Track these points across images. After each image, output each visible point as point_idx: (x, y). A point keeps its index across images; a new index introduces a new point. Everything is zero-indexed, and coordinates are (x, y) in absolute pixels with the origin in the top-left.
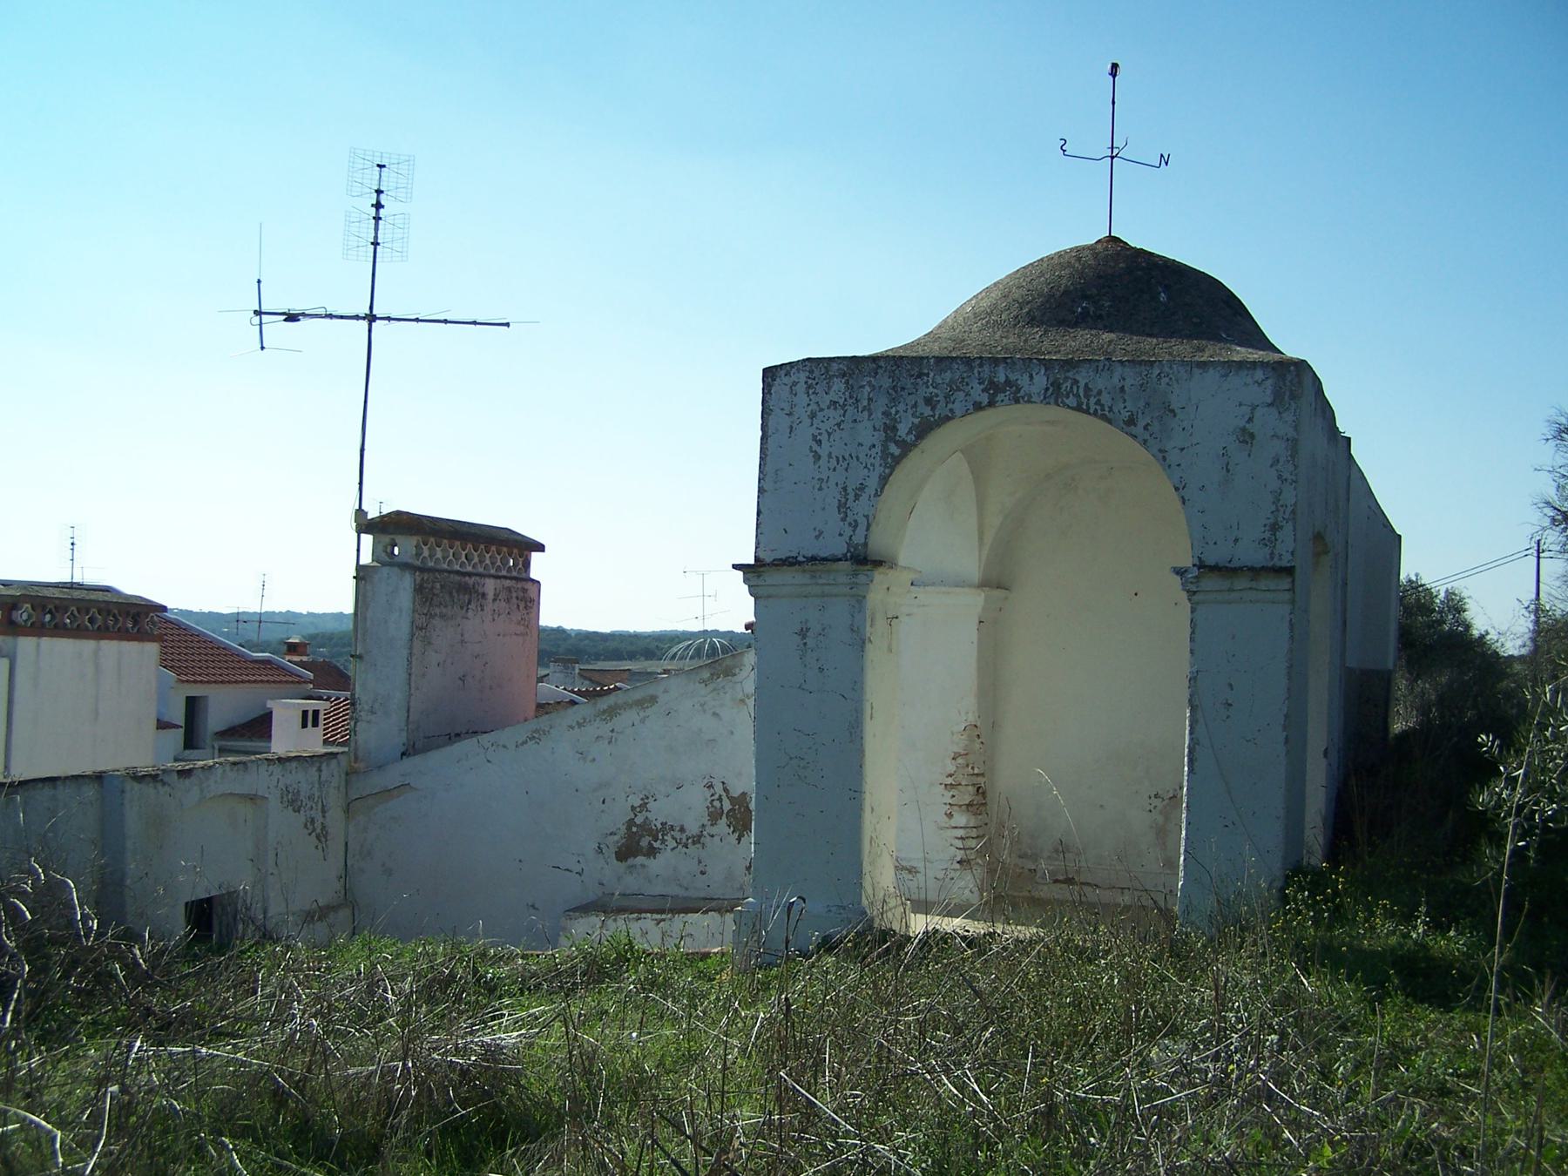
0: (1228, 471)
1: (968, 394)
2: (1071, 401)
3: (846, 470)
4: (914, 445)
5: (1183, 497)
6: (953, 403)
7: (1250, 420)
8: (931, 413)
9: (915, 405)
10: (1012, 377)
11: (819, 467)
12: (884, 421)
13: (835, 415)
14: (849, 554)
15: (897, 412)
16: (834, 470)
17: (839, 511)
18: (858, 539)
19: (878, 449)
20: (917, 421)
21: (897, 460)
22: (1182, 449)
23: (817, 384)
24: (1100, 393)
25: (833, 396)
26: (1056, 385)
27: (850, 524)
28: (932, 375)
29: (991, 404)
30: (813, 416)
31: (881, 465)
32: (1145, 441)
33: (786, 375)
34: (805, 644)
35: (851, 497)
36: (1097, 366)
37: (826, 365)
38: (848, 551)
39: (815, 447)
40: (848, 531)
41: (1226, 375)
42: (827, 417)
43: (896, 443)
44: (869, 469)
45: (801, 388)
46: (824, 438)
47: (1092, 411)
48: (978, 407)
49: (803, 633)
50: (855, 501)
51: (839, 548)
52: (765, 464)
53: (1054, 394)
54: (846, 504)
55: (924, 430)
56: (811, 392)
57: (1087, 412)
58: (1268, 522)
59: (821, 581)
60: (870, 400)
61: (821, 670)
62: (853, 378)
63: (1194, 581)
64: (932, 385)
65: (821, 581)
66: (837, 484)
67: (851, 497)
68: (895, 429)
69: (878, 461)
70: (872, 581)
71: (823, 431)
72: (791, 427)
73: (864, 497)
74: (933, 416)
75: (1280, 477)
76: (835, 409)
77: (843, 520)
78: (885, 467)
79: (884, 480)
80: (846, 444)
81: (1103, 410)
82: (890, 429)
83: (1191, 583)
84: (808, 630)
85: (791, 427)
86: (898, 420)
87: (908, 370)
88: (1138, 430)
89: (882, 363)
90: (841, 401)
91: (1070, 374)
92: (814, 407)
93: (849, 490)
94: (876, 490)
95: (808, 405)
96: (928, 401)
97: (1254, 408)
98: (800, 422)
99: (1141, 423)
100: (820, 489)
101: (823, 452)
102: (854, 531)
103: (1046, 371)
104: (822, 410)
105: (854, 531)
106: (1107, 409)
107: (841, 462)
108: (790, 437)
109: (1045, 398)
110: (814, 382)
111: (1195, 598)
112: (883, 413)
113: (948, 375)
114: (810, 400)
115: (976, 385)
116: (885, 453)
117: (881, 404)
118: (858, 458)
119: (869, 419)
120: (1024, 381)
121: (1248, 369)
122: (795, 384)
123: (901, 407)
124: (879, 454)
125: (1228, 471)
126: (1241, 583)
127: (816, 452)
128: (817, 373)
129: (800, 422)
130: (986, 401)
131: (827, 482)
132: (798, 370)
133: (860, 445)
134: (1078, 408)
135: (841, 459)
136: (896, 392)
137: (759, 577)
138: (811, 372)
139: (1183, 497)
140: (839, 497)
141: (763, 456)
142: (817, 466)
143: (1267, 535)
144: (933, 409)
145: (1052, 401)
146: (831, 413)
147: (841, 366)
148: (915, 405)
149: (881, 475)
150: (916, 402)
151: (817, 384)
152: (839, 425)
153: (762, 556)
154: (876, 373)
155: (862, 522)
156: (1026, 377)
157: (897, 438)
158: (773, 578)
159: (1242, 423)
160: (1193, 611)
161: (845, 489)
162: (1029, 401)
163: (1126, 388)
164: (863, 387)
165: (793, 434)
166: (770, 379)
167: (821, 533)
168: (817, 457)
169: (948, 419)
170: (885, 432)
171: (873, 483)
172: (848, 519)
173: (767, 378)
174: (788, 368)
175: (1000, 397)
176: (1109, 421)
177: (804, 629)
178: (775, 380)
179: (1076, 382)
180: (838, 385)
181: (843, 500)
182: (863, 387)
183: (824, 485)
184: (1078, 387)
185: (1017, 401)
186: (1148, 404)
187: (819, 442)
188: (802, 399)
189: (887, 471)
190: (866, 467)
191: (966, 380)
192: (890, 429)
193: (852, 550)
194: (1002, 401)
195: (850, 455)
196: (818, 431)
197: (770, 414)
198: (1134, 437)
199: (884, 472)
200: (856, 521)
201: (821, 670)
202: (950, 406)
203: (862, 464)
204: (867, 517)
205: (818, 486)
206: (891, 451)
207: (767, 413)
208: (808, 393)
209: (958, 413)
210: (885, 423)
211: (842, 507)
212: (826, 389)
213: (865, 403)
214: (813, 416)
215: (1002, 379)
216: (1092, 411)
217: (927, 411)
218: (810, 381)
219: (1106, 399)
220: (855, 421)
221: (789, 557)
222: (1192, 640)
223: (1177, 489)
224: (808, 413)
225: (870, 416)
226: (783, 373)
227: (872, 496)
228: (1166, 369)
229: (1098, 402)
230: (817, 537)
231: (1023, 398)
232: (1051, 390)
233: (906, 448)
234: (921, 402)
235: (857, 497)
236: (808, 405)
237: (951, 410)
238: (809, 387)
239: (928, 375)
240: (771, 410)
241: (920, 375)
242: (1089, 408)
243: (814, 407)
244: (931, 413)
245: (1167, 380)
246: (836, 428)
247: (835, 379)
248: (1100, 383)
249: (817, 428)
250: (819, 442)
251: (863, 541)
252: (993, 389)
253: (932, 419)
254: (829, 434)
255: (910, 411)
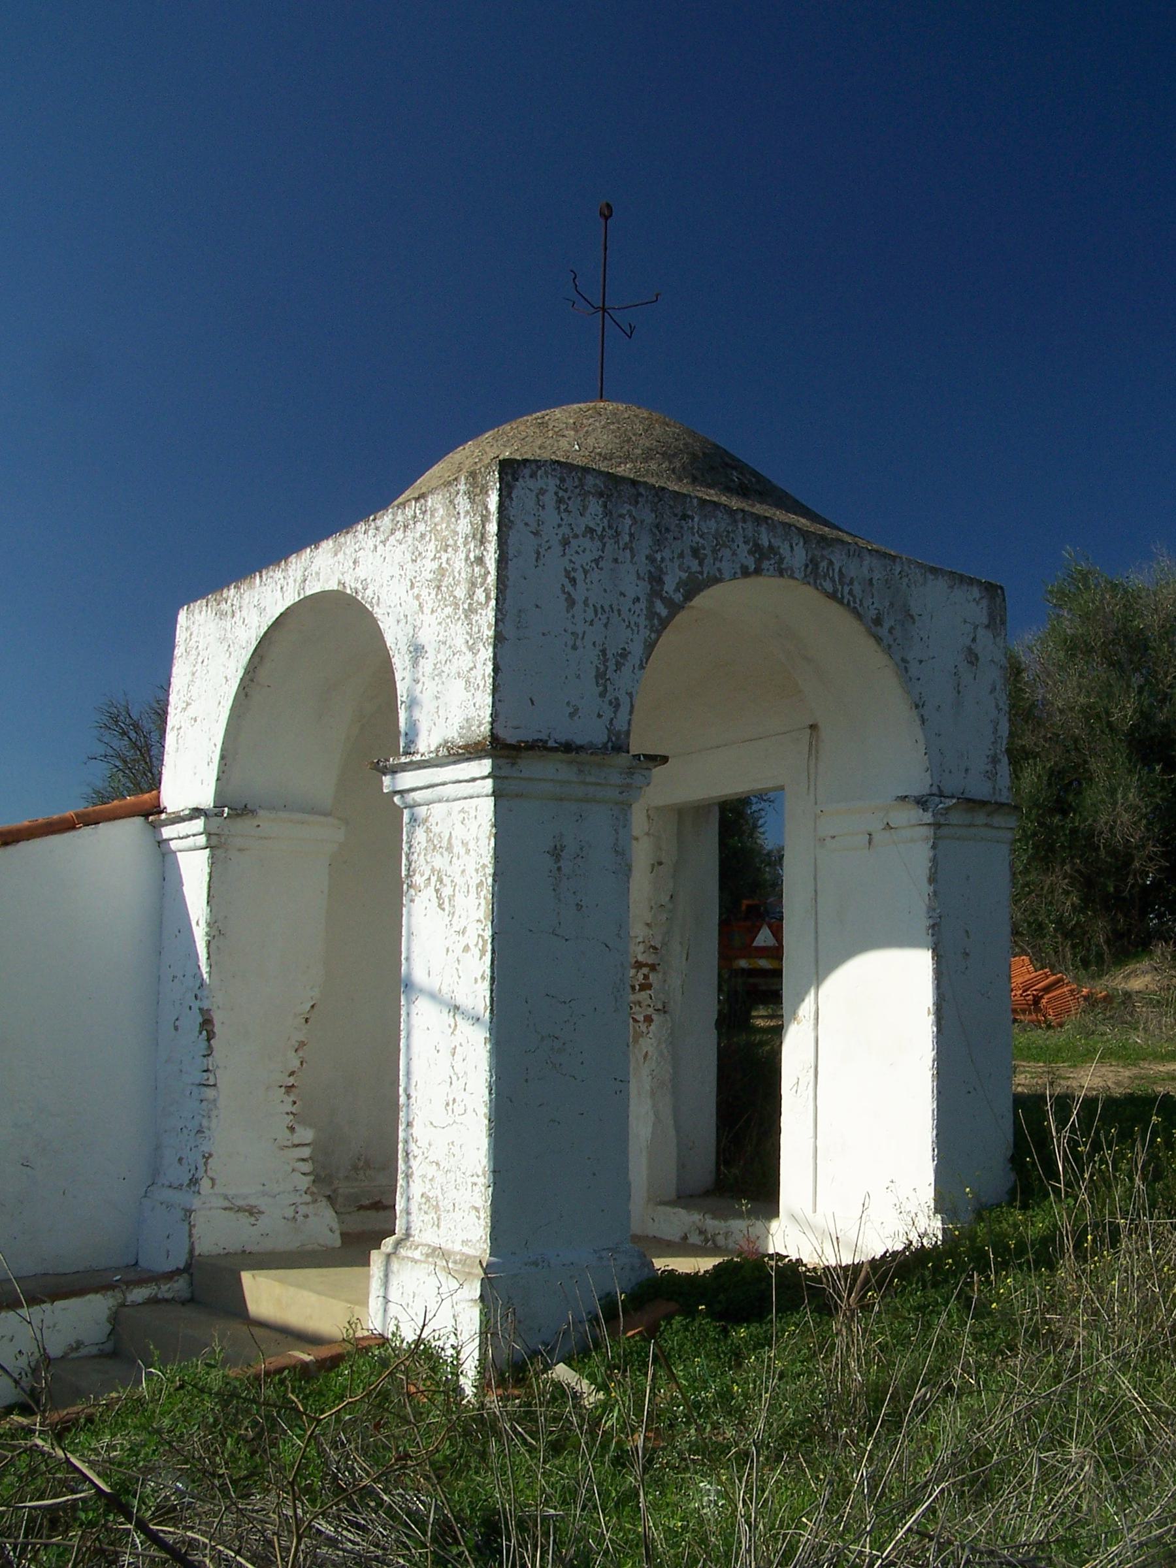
0: (959, 692)
1: (734, 554)
2: (828, 586)
3: (606, 625)
4: (681, 607)
5: (922, 716)
6: (721, 561)
7: (974, 640)
8: (699, 569)
9: (681, 555)
10: (776, 542)
11: (573, 617)
12: (649, 568)
13: (591, 547)
14: (610, 744)
15: (663, 559)
16: (591, 624)
17: (597, 683)
18: (620, 724)
19: (643, 604)
20: (684, 575)
21: (665, 623)
22: (921, 662)
23: (569, 498)
24: (851, 582)
25: (587, 521)
26: (814, 563)
27: (610, 703)
28: (696, 519)
29: (758, 571)
30: (565, 543)
31: (646, 627)
32: (890, 646)
33: (531, 477)
34: (559, 869)
35: (611, 665)
36: (849, 550)
37: (579, 474)
38: (610, 739)
39: (569, 588)
40: (608, 713)
41: (951, 587)
42: (582, 548)
43: (663, 599)
44: (632, 630)
45: (549, 499)
46: (579, 576)
47: (845, 601)
48: (746, 573)
49: (556, 853)
50: (616, 671)
51: (600, 737)
52: (505, 599)
53: (813, 573)
54: (605, 674)
55: (692, 588)
56: (563, 507)
57: (840, 602)
58: (989, 753)
59: (588, 779)
60: (631, 535)
61: (579, 907)
62: (611, 501)
63: (944, 812)
64: (698, 532)
65: (589, 779)
66: (594, 644)
67: (611, 665)
68: (660, 581)
69: (642, 621)
70: (648, 784)
71: (577, 566)
72: (538, 553)
73: (626, 670)
74: (701, 573)
75: (997, 706)
76: (592, 539)
77: (602, 695)
78: (652, 631)
79: (650, 646)
80: (605, 591)
81: (855, 602)
82: (656, 580)
83: (941, 814)
84: (563, 848)
85: (538, 553)
86: (665, 570)
87: (671, 507)
88: (883, 632)
89: (642, 490)
90: (599, 530)
91: (825, 553)
92: (565, 530)
93: (610, 655)
94: (641, 661)
95: (559, 526)
96: (695, 552)
97: (976, 627)
98: (549, 548)
99: (886, 626)
100: (574, 647)
101: (579, 595)
102: (615, 712)
103: (805, 543)
104: (576, 536)
105: (615, 712)
106: (858, 602)
107: (599, 615)
108: (536, 567)
109: (806, 576)
110: (566, 496)
111: (944, 831)
112: (647, 558)
113: (712, 524)
114: (562, 519)
115: (742, 545)
116: (652, 614)
117: (644, 544)
118: (619, 611)
119: (631, 562)
120: (784, 550)
121: (968, 584)
122: (542, 492)
123: (667, 553)
124: (645, 612)
125: (959, 692)
126: (981, 818)
127: (569, 594)
128: (569, 484)
129: (549, 548)
130: (752, 567)
131: (583, 638)
132: (546, 472)
133: (622, 594)
134: (833, 596)
135: (600, 610)
136: (660, 532)
137: (513, 764)
138: (562, 480)
139: (922, 716)
140: (596, 662)
141: (501, 586)
142: (570, 615)
143: (989, 767)
144: (701, 564)
145: (812, 581)
146: (586, 542)
147: (598, 482)
148: (681, 555)
149: (646, 641)
150: (682, 551)
151: (569, 498)
152: (597, 561)
153: (502, 734)
154: (637, 502)
155: (625, 700)
156: (787, 546)
157: (665, 595)
158: (533, 768)
159: (968, 642)
160: (934, 847)
161: (604, 652)
162: (792, 577)
163: (874, 582)
164: (622, 516)
165: (541, 563)
166: (510, 477)
167: (577, 710)
168: (571, 602)
169: (717, 580)
170: (650, 583)
171: (637, 649)
172: (608, 694)
173: (506, 474)
174: (534, 466)
175: (765, 564)
176: (859, 616)
177: (558, 847)
178: (517, 480)
179: (831, 563)
180: (595, 506)
181: (602, 668)
182: (622, 516)
183: (579, 643)
184: (833, 570)
185: (781, 573)
186: (892, 605)
187: (573, 581)
188: (551, 516)
189: (653, 636)
190: (628, 627)
191: (731, 535)
192: (656, 580)
193: (614, 739)
194: (768, 570)
195: (611, 606)
196: (572, 565)
197: (510, 527)
198: (878, 640)
199: (649, 636)
200: (617, 699)
201: (579, 907)
202: (718, 564)
203: (624, 621)
204: (630, 695)
205: (570, 643)
206: (658, 611)
207: (506, 525)
208: (559, 507)
209: (726, 575)
210: (650, 572)
211: (600, 676)
212: (581, 508)
213: (627, 538)
214: (565, 543)
215: (766, 544)
216: (845, 601)
217: (695, 565)
218: (561, 493)
219: (857, 588)
220: (616, 560)
221: (537, 741)
222: (932, 880)
223: (917, 706)
224: (560, 537)
225: (632, 558)
226: (527, 472)
227: (636, 666)
228: (906, 568)
229: (851, 592)
230: (572, 715)
231: (786, 570)
232: (810, 566)
233: (675, 608)
234: (688, 552)
235: (619, 666)
236: (559, 526)
237: (719, 570)
238: (560, 501)
239: (693, 519)
240: (512, 522)
241: (685, 517)
242: (843, 597)
243: (565, 530)
244: (699, 569)
245: (906, 580)
246: (593, 565)
247: (591, 497)
248: (852, 570)
249: (571, 561)
250: (573, 581)
251: (625, 728)
252: (761, 553)
253: (700, 577)
254: (586, 572)
255: (677, 563)
